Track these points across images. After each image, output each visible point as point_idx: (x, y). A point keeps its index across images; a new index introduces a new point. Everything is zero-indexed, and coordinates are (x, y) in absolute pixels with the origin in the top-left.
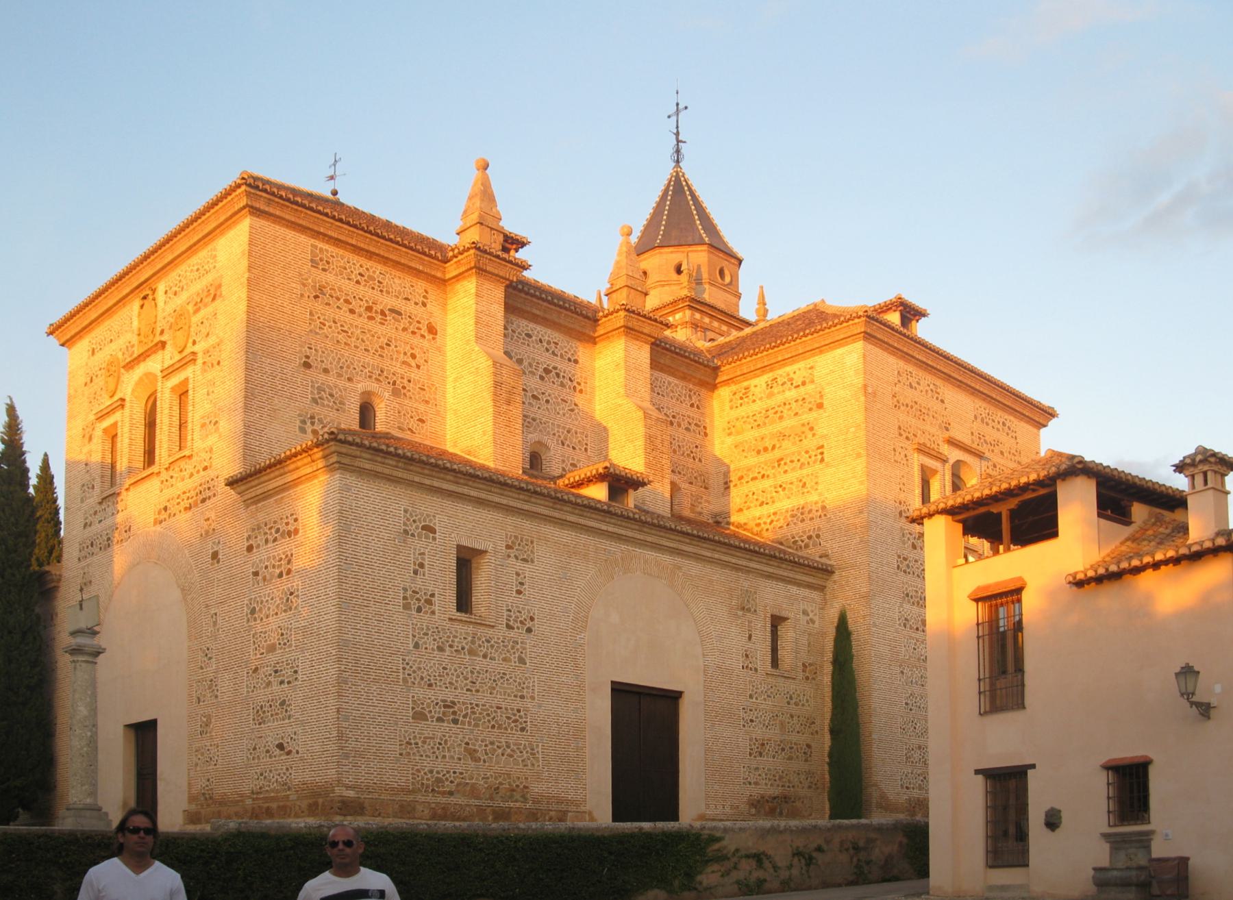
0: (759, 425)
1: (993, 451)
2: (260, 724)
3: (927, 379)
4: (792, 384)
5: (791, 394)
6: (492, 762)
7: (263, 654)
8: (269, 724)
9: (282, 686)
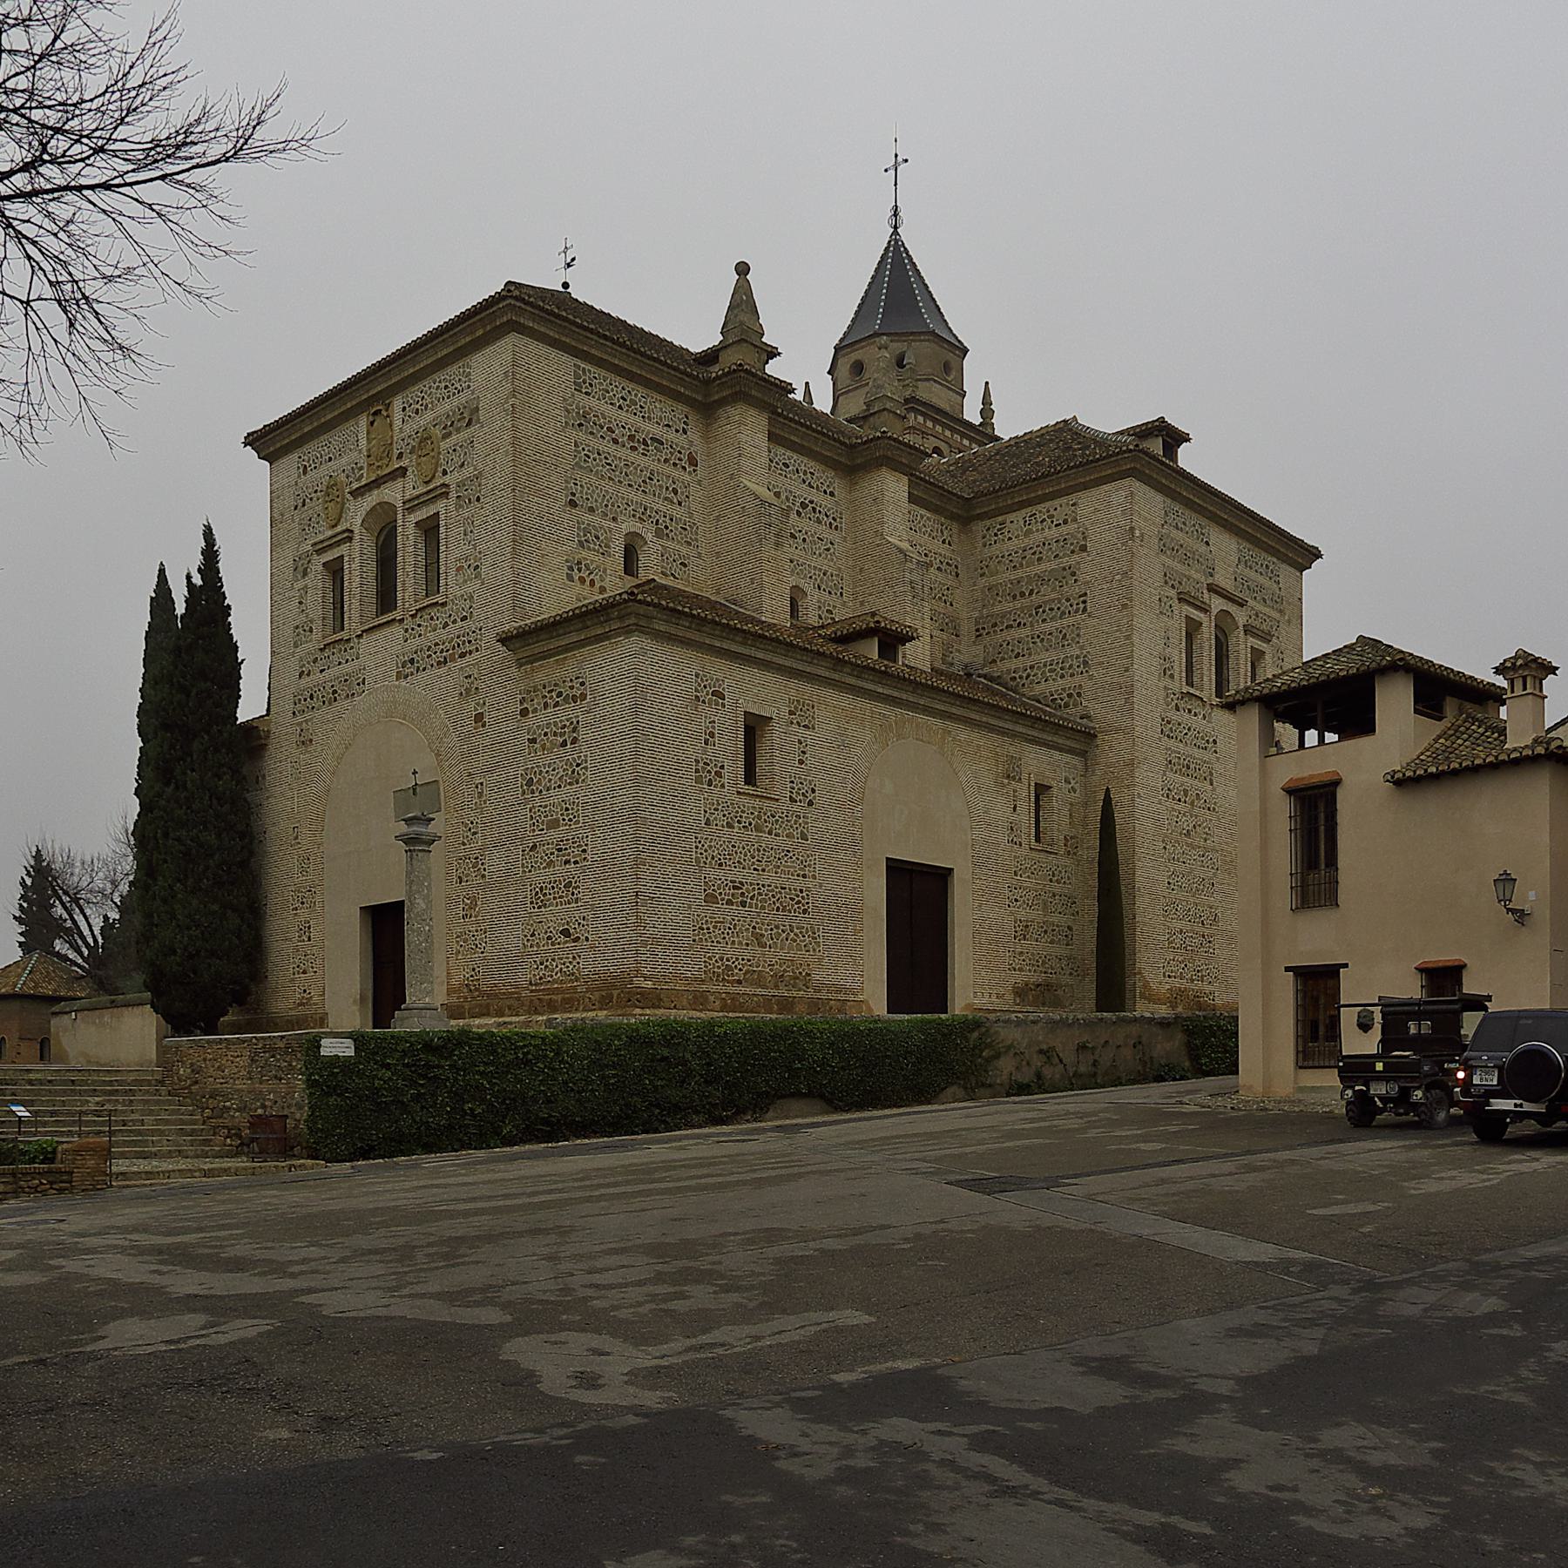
0: (1015, 566)
1: (1255, 598)
3: (1193, 519)
4: (1052, 522)
5: (1052, 533)
6: (776, 948)
7: (543, 830)
9: (567, 866)
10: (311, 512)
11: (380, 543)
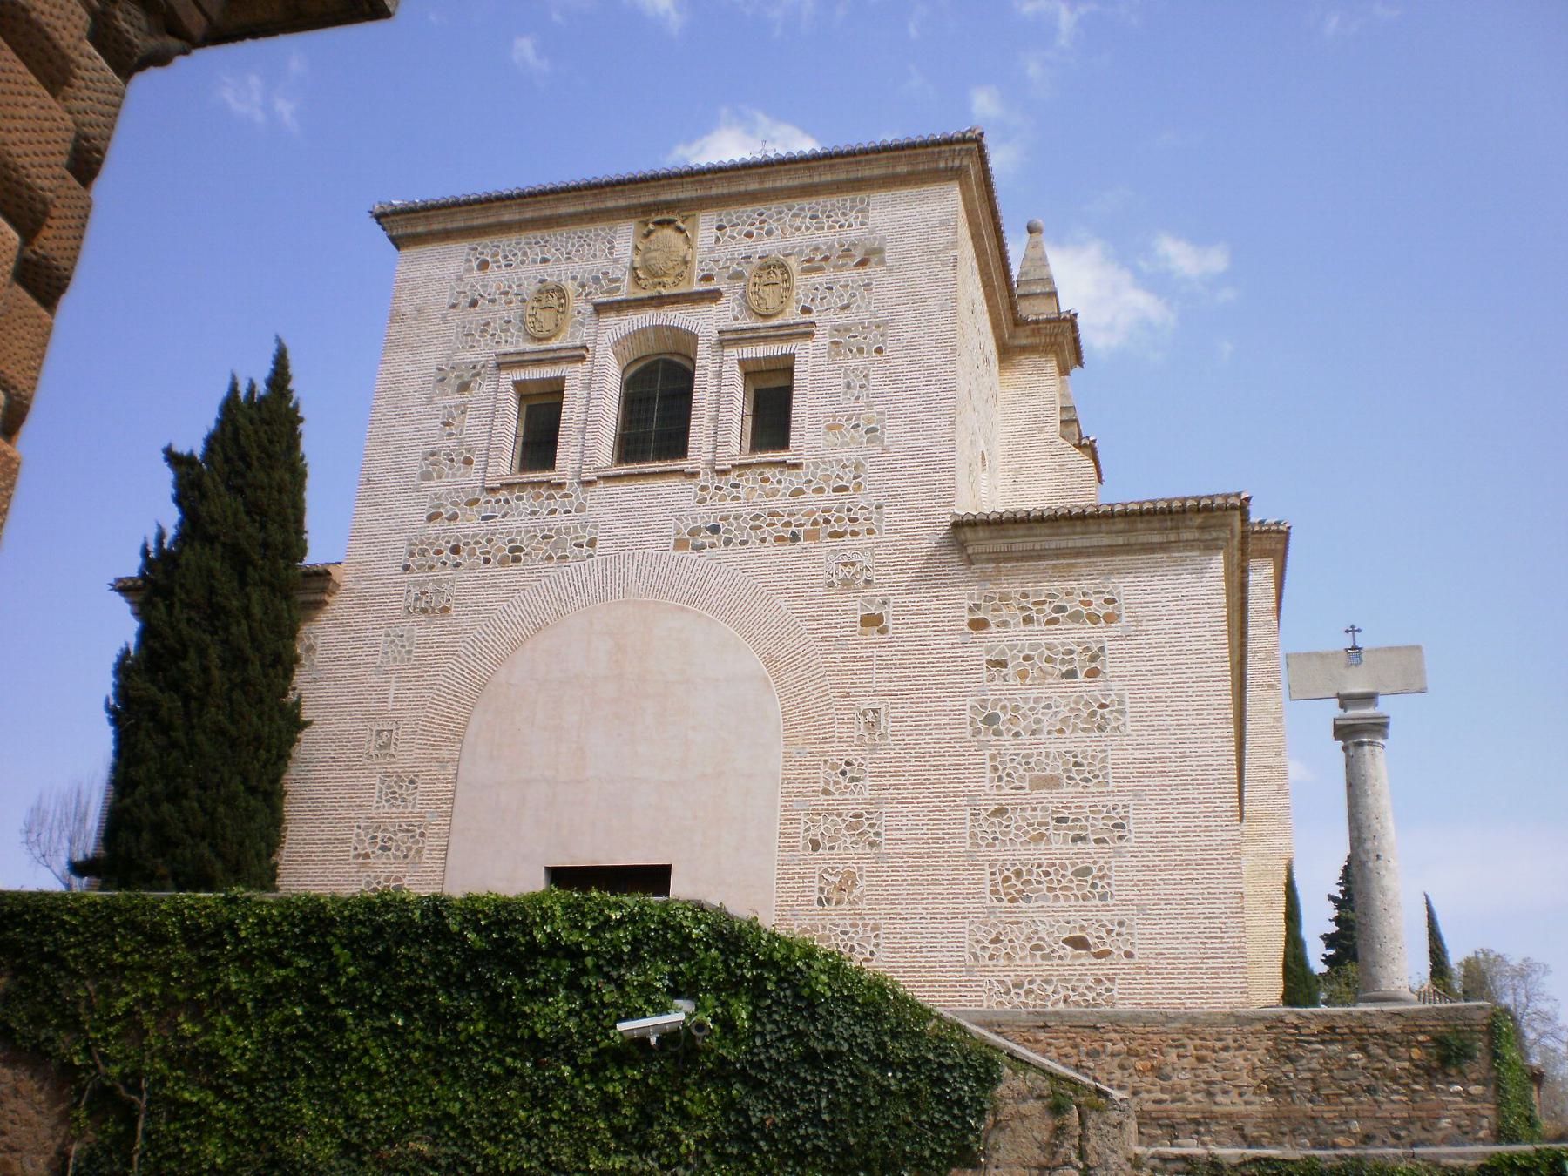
2: (1013, 900)
8: (1040, 903)
9: (1080, 844)
10: (486, 316)
11: (627, 376)
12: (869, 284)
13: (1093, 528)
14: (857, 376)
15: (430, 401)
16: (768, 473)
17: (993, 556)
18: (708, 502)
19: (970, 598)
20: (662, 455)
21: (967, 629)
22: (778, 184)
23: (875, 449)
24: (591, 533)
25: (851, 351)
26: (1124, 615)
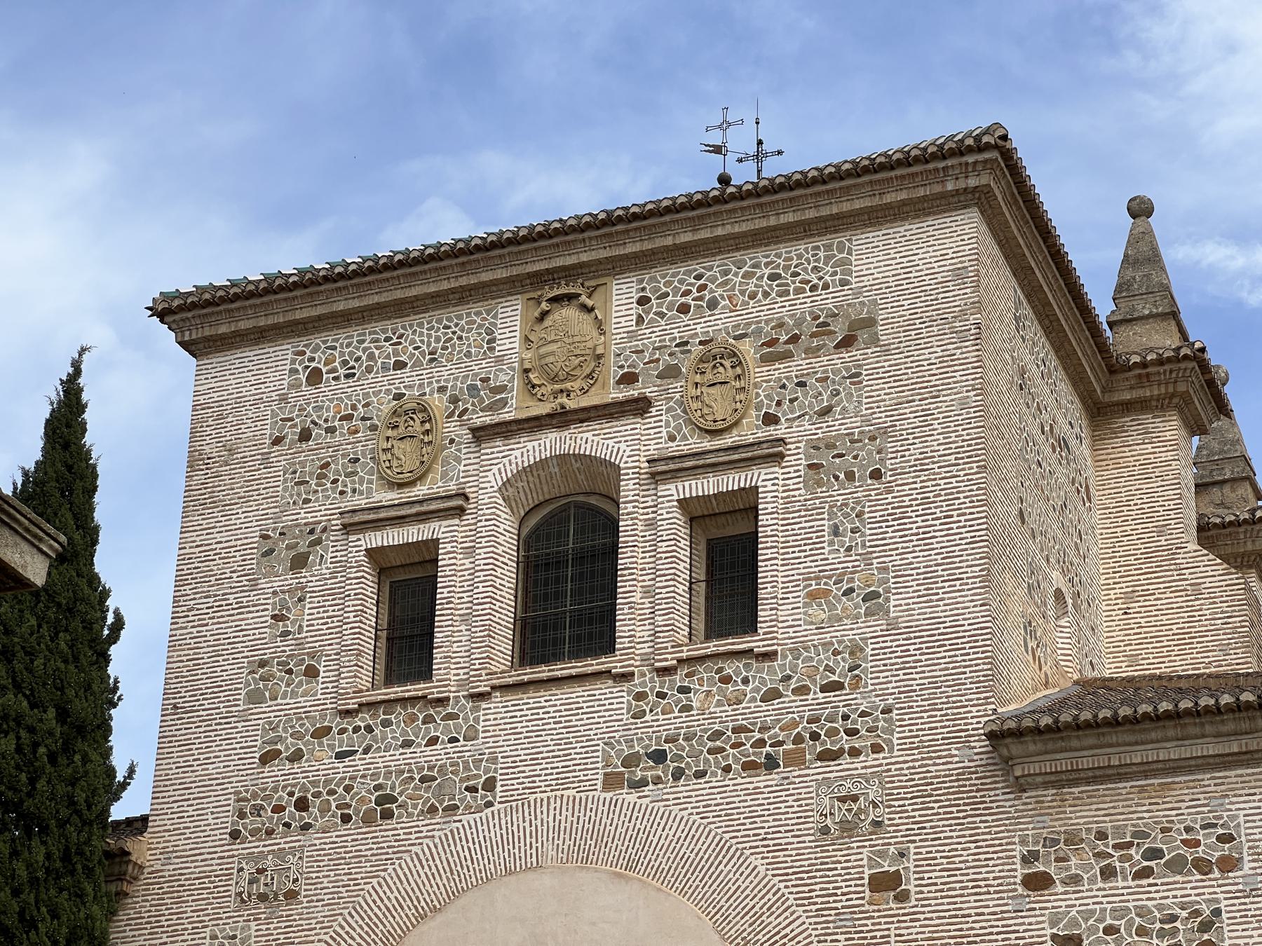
11: (525, 531)
12: (858, 375)
13: (1193, 730)
14: (846, 515)
15: (254, 584)
16: (729, 668)
17: (1053, 778)
18: (648, 717)
19: (1023, 842)
20: (579, 653)
21: (1020, 890)
22: (720, 232)
23: (879, 625)
24: (487, 771)
25: (836, 478)
26: (1246, 858)
